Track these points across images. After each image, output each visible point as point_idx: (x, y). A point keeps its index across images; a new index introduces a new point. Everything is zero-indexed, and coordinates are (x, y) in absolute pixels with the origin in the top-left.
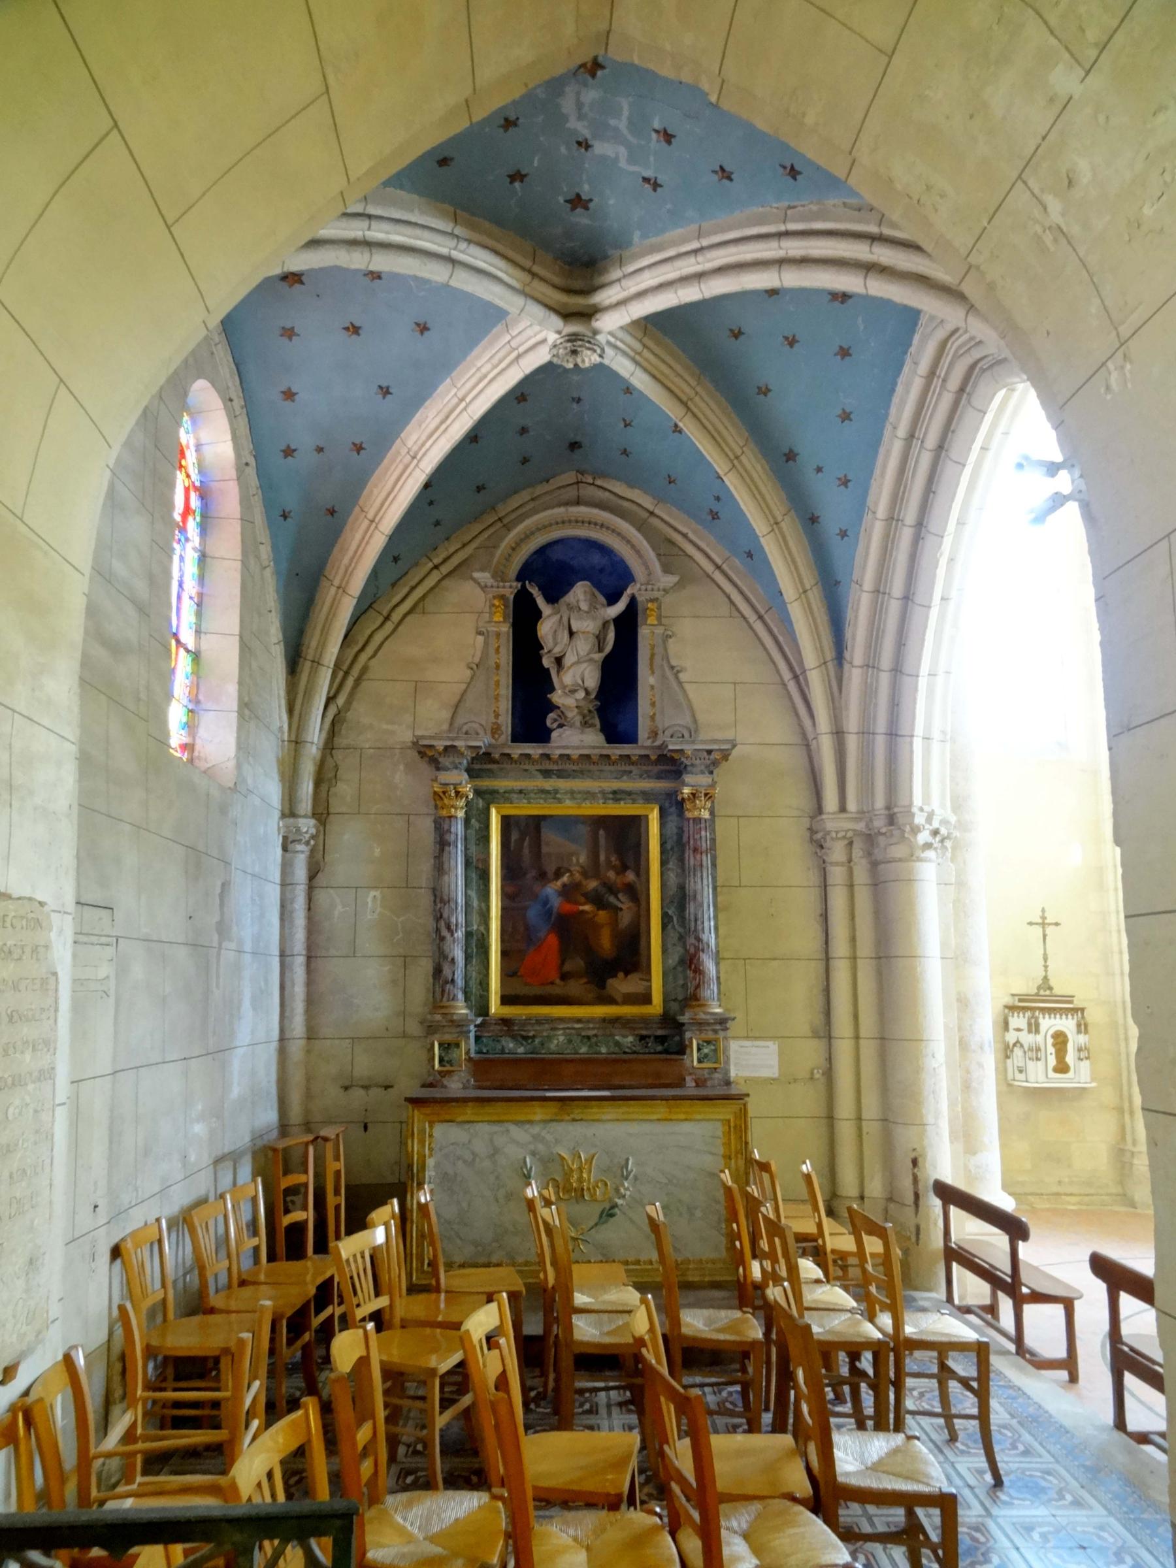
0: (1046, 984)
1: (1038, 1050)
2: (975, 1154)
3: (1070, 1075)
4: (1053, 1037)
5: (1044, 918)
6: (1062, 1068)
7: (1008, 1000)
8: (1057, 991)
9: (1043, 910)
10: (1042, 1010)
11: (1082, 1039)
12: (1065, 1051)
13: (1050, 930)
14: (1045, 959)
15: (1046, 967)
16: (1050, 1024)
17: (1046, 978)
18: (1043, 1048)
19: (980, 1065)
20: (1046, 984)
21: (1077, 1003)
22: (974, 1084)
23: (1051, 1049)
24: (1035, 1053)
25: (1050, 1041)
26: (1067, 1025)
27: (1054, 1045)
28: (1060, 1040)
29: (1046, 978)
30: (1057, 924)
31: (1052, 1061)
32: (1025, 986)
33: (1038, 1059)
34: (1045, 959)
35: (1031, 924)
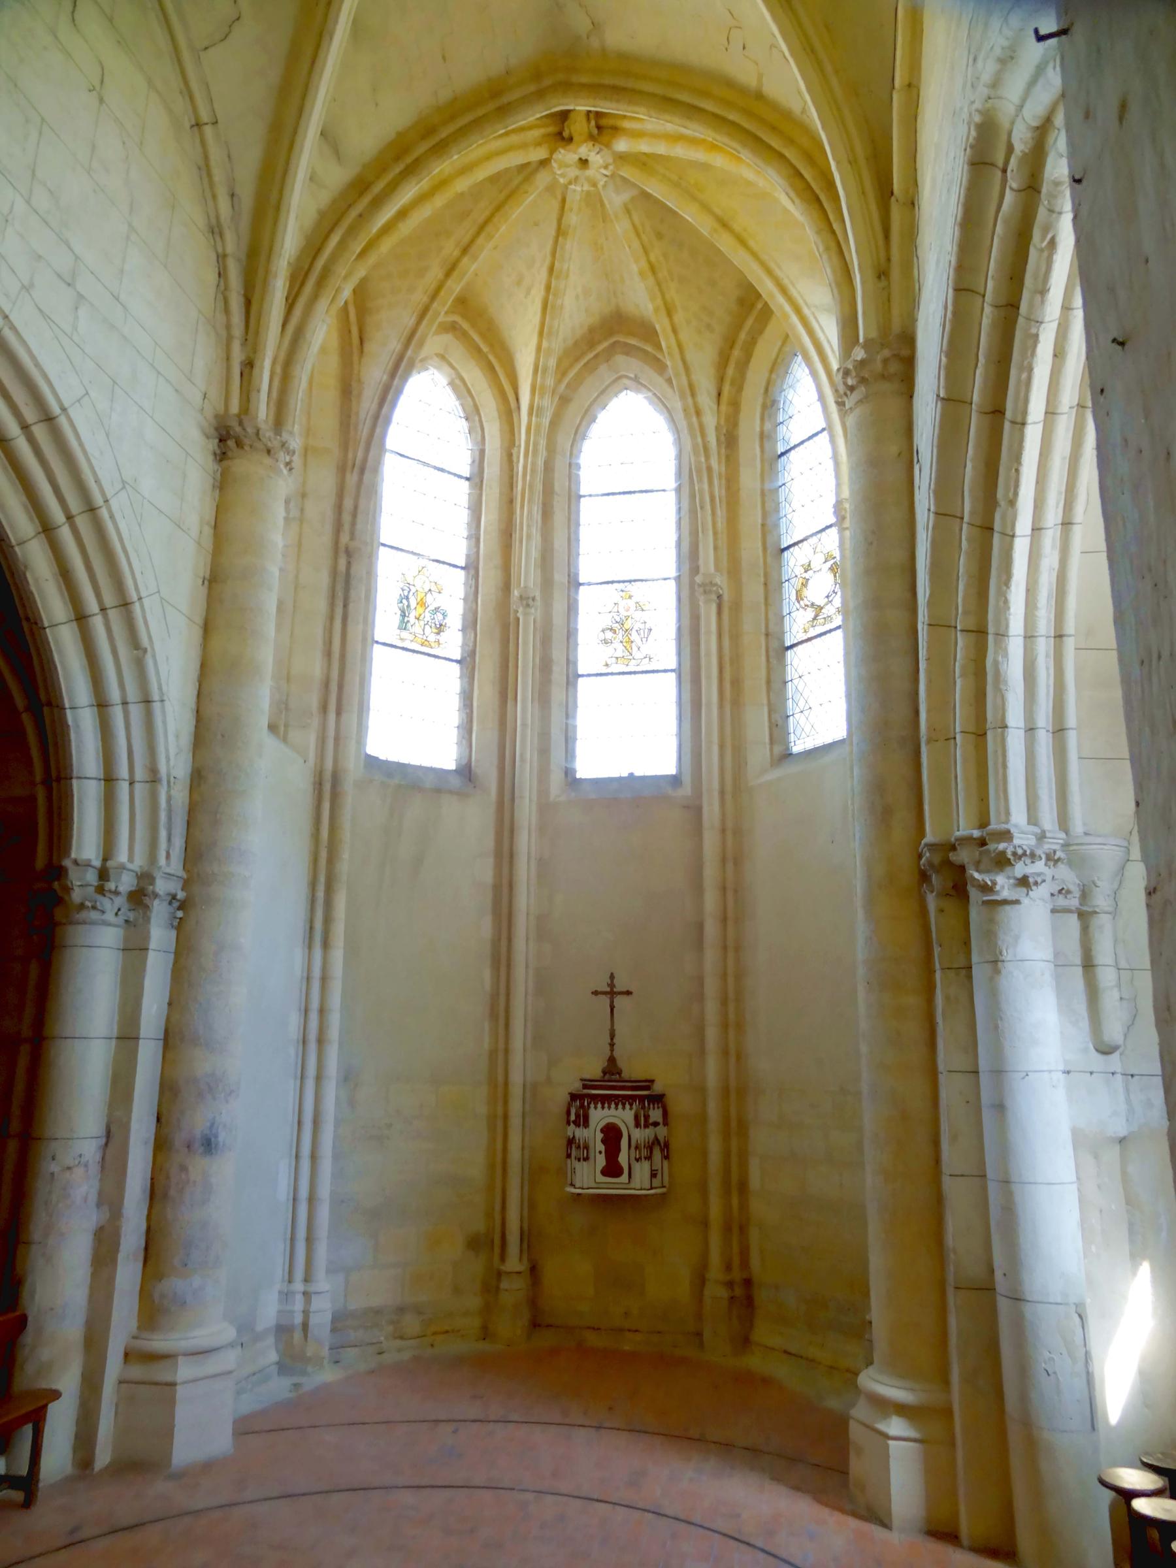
0: (612, 1068)
1: (586, 1147)
2: (159, 1277)
3: (624, 1178)
4: (602, 1131)
5: (612, 985)
6: (612, 1169)
7: (576, 1086)
8: (625, 1075)
9: (612, 977)
10: (594, 1098)
11: (639, 1135)
12: (619, 1150)
13: (619, 1001)
14: (612, 1037)
15: (612, 1045)
16: (600, 1116)
17: (612, 1060)
18: (591, 1145)
19: (183, 1168)
20: (612, 1068)
21: (658, 1088)
22: (172, 1192)
23: (602, 1148)
25: (600, 1136)
26: (623, 1116)
27: (603, 1141)
29: (612, 1060)
30: (628, 993)
31: (601, 1161)
32: (594, 1068)
33: (586, 1159)
34: (612, 1037)
35: (596, 993)
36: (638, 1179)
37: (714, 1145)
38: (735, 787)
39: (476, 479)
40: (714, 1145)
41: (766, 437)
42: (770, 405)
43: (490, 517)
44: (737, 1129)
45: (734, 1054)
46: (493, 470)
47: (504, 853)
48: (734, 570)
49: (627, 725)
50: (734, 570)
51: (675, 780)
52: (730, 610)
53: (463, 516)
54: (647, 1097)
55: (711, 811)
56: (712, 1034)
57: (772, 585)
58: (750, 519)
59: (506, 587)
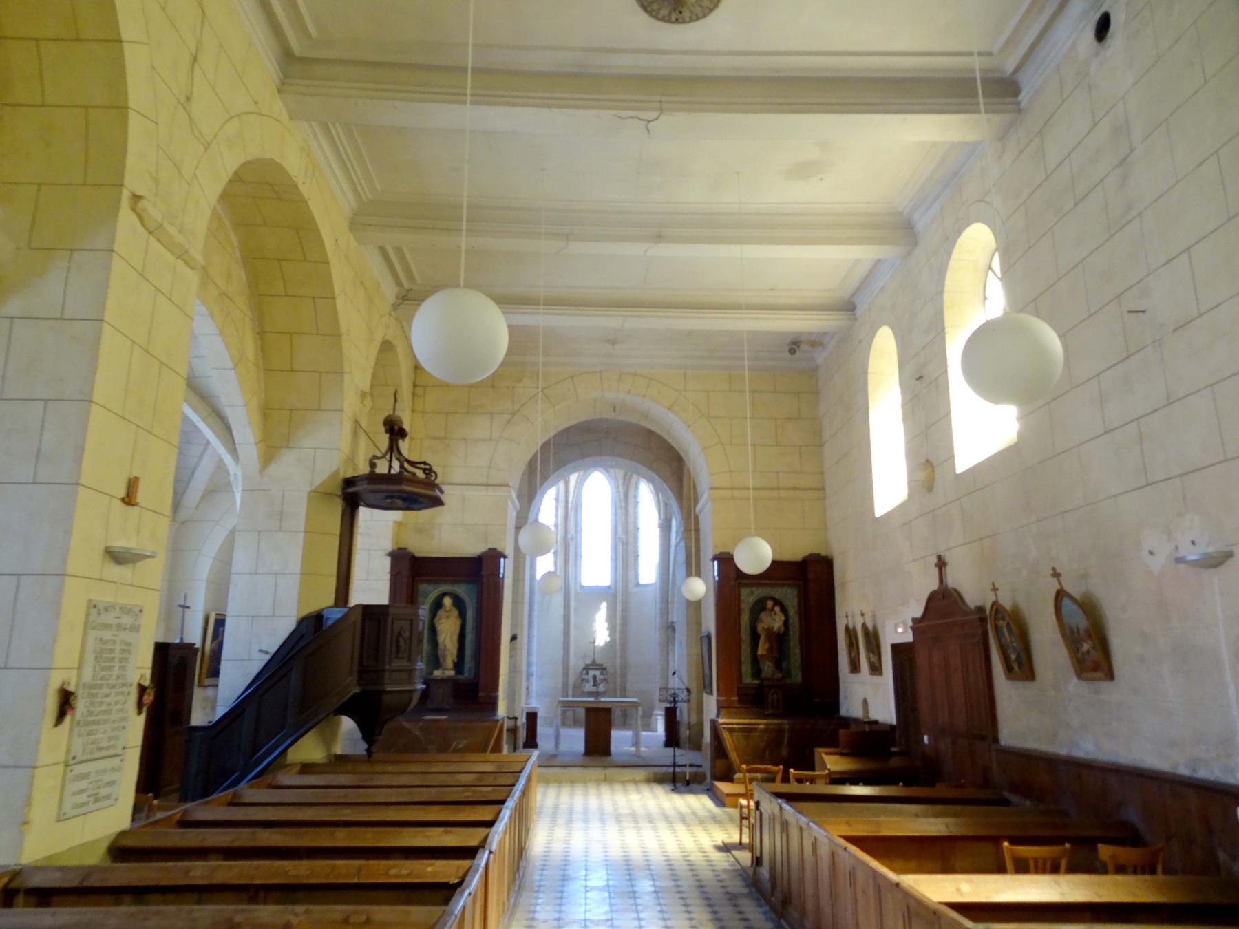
6: (595, 685)
16: (592, 673)
20: (594, 661)
24: (587, 681)
26: (597, 673)
28: (595, 677)
32: (589, 662)
36: (601, 688)
37: (619, 680)
38: (626, 594)
39: (557, 500)
40: (619, 680)
41: (636, 496)
42: (637, 488)
43: (561, 512)
44: (624, 676)
45: (623, 657)
46: (562, 498)
47: (567, 607)
48: (627, 533)
49: (596, 570)
50: (627, 533)
51: (609, 587)
52: (626, 544)
53: (554, 510)
54: (602, 669)
55: (619, 598)
56: (618, 654)
57: (636, 538)
58: (631, 519)
59: (566, 533)
